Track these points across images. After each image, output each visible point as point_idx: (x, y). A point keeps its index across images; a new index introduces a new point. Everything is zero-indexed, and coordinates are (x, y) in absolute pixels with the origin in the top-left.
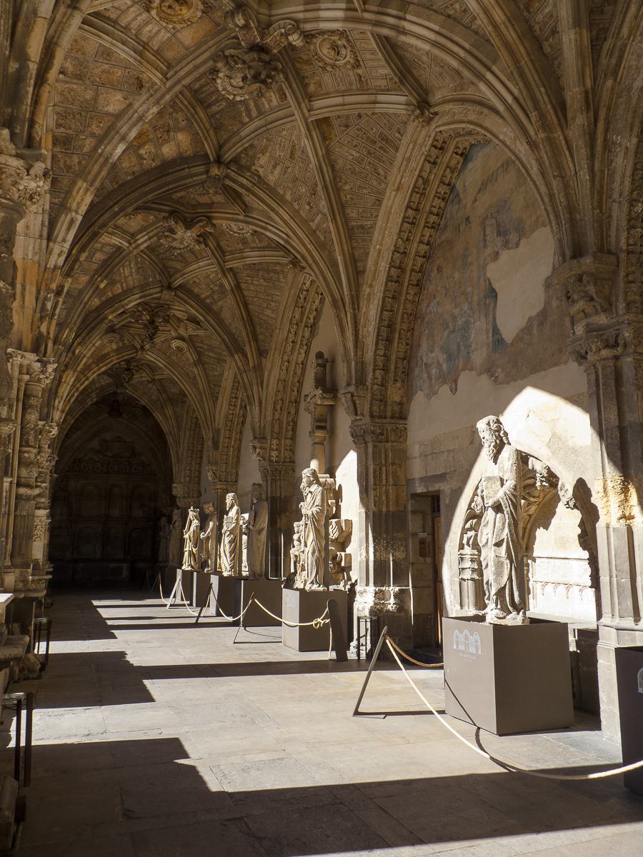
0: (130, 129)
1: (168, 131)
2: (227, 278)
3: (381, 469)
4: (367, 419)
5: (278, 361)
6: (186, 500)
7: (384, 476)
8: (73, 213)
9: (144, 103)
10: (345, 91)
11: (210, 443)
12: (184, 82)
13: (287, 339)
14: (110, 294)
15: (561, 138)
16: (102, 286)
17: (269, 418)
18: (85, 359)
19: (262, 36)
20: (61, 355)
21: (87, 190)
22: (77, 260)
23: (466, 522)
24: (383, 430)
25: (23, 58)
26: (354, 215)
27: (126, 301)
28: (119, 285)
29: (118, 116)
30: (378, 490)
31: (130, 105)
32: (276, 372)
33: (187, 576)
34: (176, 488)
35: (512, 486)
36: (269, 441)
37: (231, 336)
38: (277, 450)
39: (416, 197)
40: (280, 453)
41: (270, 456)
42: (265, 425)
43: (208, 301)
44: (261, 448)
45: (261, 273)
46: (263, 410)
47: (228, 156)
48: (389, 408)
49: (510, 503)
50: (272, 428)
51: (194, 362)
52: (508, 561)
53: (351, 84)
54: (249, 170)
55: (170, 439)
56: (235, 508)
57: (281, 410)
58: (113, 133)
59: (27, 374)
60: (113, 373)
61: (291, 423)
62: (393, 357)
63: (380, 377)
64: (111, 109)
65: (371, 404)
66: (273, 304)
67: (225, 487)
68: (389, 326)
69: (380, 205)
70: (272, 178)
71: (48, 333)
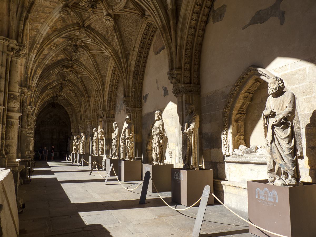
0: (49, 58)
4: (106, 118)
5: (93, 100)
6: (75, 134)
8: (37, 75)
11: (80, 118)
12: (61, 49)
13: (95, 94)
14: (49, 82)
16: (46, 81)
17: (91, 114)
18: (43, 96)
19: (76, 43)
20: (36, 99)
21: (40, 70)
22: (38, 84)
25: (27, 74)
26: (102, 73)
27: (53, 84)
28: (51, 80)
29: (47, 55)
31: (49, 52)
32: (93, 102)
33: (73, 154)
37: (82, 92)
38: (93, 122)
39: (114, 71)
43: (75, 83)
44: (89, 121)
45: (88, 78)
47: (73, 59)
48: (111, 116)
53: (97, 48)
55: (70, 116)
56: (84, 137)
58: (46, 58)
59: (28, 110)
60: (53, 97)
62: (112, 104)
63: (108, 109)
64: (45, 53)
65: (107, 115)
66: (91, 85)
68: (110, 98)
70: (84, 63)
71: (33, 101)
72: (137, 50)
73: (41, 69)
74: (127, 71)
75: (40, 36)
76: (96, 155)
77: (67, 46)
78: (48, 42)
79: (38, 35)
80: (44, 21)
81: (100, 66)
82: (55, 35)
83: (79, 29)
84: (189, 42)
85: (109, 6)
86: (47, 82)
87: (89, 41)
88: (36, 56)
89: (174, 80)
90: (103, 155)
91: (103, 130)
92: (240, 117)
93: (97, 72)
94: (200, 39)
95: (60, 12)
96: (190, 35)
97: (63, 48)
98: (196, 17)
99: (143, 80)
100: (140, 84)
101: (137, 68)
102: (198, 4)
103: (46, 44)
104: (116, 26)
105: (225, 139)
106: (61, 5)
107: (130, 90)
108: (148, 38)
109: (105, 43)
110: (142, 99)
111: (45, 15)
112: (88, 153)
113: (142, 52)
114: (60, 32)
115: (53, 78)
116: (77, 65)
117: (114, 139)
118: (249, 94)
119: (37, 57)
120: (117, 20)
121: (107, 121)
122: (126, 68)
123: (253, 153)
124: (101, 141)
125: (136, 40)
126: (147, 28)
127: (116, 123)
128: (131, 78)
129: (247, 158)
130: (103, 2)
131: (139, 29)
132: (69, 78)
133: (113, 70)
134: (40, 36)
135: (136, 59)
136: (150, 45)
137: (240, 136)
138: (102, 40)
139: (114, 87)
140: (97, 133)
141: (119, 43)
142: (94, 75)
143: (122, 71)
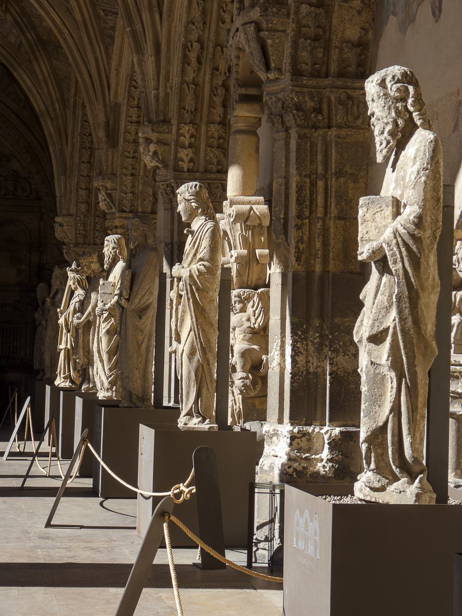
3: (313, 185)
4: (287, 78)
7: (320, 200)
11: (101, 134)
17: (175, 80)
24: (320, 102)
30: (306, 229)
34: (61, 225)
35: (412, 218)
36: (174, 128)
38: (190, 146)
40: (197, 153)
41: (177, 159)
42: (167, 95)
44: (159, 142)
46: (163, 63)
48: (335, 55)
49: (404, 253)
50: (181, 99)
52: (393, 374)
55: (49, 127)
56: (120, 265)
57: (199, 62)
61: (221, 91)
76: (194, 423)
90: (262, 417)
91: (265, 208)
112: (144, 398)
117: (384, 268)
121: (298, 107)
124: (248, 299)
127: (408, 79)
140: (210, 224)
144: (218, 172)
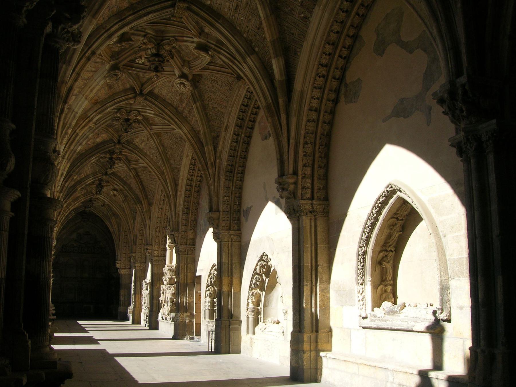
0: (83, 141)
1: (99, 135)
2: (132, 172)
9: (88, 132)
10: (163, 123)
13: (160, 198)
14: (79, 179)
15: (208, 173)
19: (128, 116)
21: (68, 162)
22: (64, 186)
23: (207, 288)
43: (125, 179)
47: (123, 141)
51: (123, 201)
54: (132, 143)
67: (140, 265)
69: (182, 160)
70: (142, 146)
72: (231, 130)
73: (69, 161)
74: (214, 167)
75: (72, 116)
77: (112, 121)
78: (85, 123)
79: (70, 114)
80: (79, 92)
81: (169, 151)
82: (95, 110)
83: (135, 97)
84: (309, 132)
85: (184, 61)
86: (76, 178)
87: (150, 113)
88: (65, 147)
89: (285, 193)
92: (386, 255)
93: (163, 161)
94: (327, 127)
95: (105, 77)
96: (310, 122)
97: (106, 124)
98: (318, 94)
99: (242, 183)
100: (237, 188)
101: (233, 161)
102: (321, 74)
103: (81, 127)
104: (195, 92)
105: (361, 292)
106: (107, 67)
107: (221, 198)
108: (250, 111)
109: (178, 119)
110: (240, 214)
111: (82, 82)
113: (240, 134)
114: (104, 105)
115: (86, 171)
116: (129, 150)
118: (397, 221)
119: (66, 149)
120: (198, 82)
122: (212, 160)
123: (396, 315)
125: (230, 114)
126: (247, 96)
128: (223, 179)
129: (388, 322)
130: (175, 57)
131: (234, 98)
132: (114, 170)
133: (192, 158)
134: (72, 116)
135: (231, 146)
136: (254, 121)
137: (385, 286)
138: (173, 114)
139: (193, 189)
141: (201, 119)
142: (159, 167)
143: (206, 165)
144: (164, 256)
